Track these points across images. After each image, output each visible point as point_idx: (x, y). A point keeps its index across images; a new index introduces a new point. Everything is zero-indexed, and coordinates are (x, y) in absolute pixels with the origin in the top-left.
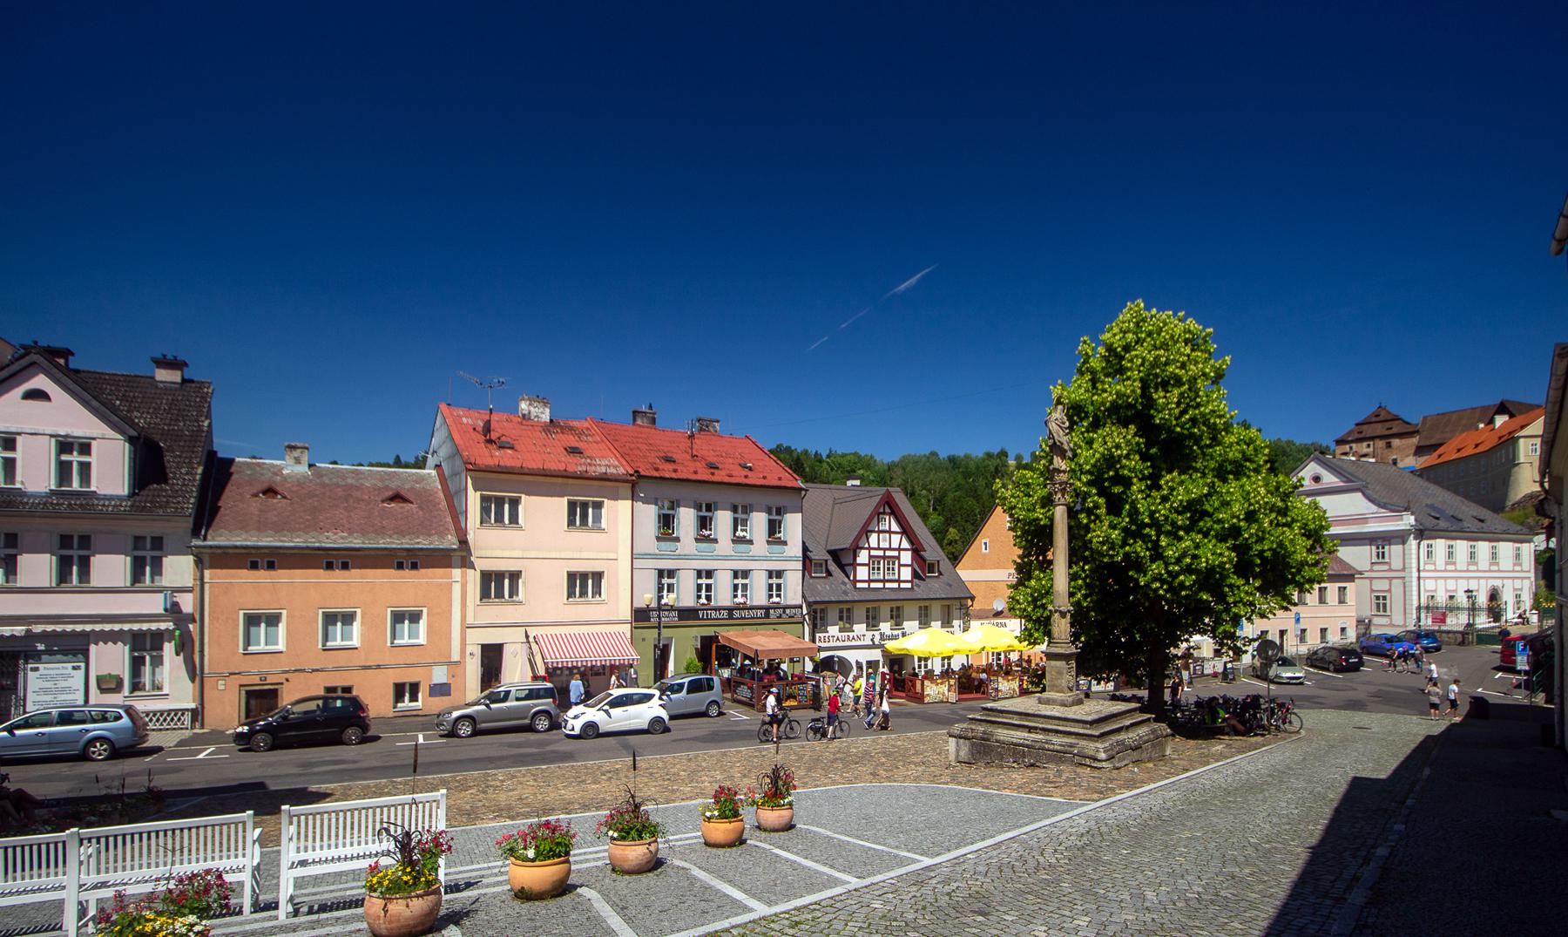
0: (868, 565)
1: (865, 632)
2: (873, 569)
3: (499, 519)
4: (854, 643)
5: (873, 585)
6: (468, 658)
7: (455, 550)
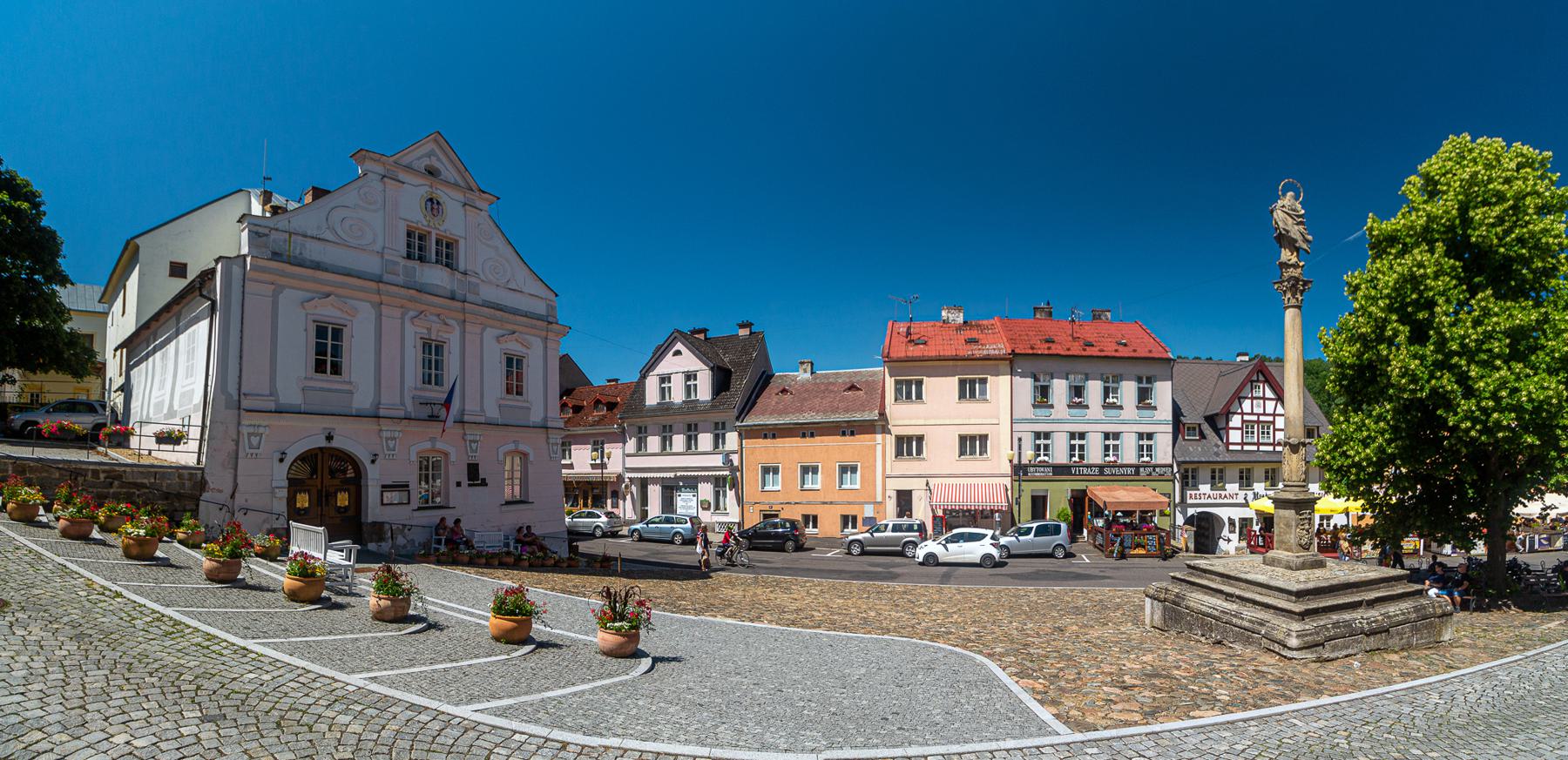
0: (1241, 429)
1: (1237, 491)
2: (1247, 432)
3: (909, 396)
4: (1226, 501)
5: (1246, 448)
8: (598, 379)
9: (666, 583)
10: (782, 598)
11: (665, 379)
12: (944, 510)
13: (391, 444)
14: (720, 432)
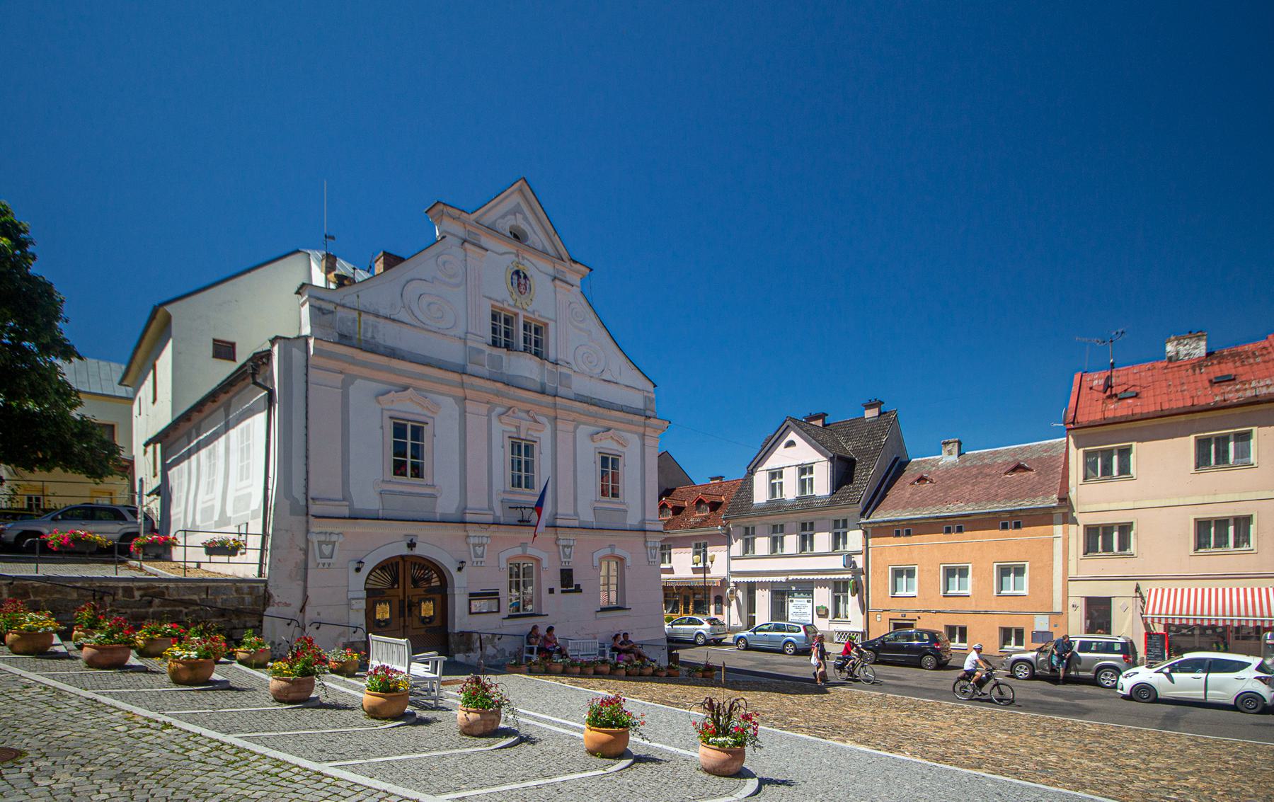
6: (1071, 609)
7: (1054, 507)
8: (700, 477)
9: (775, 696)
10: (921, 725)
11: (776, 474)
12: (1167, 626)
13: (479, 550)
14: (841, 531)
